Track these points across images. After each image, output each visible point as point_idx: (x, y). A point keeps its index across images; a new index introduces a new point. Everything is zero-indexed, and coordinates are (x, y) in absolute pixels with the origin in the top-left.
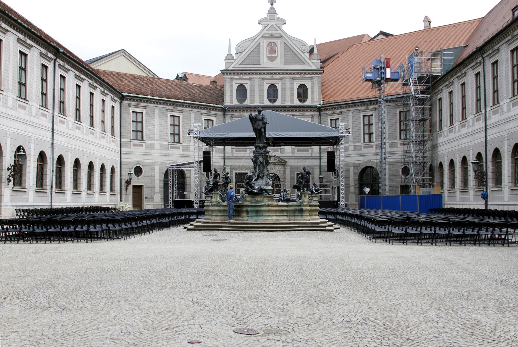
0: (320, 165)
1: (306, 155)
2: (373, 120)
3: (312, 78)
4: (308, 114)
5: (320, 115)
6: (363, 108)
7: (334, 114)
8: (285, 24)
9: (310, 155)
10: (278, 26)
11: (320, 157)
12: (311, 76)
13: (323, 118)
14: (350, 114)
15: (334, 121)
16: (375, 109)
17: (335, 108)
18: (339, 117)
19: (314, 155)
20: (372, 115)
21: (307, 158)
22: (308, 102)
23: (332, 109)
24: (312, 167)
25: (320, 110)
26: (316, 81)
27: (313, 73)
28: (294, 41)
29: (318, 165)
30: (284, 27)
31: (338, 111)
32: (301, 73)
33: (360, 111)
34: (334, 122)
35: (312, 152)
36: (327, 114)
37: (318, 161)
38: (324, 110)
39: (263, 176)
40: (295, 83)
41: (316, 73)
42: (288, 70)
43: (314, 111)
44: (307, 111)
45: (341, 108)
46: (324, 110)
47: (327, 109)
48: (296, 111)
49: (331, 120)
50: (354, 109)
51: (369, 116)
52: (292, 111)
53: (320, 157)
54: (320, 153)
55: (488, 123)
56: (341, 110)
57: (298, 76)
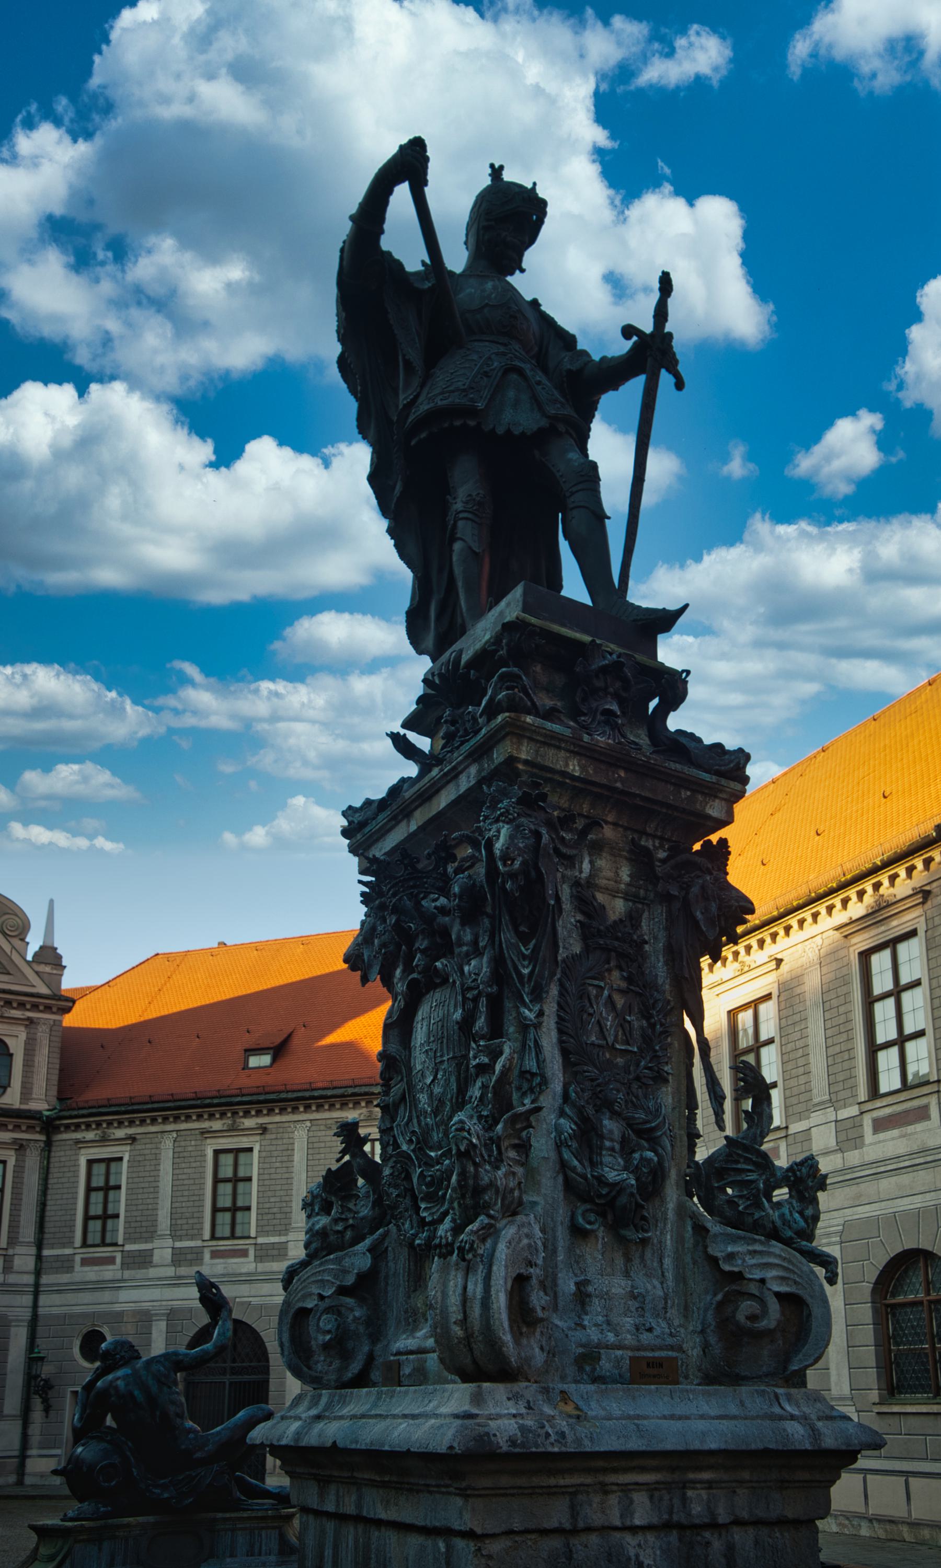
0: (35, 1318)
2: (254, 1166)
6: (217, 1125)
7: (104, 1140)
11: (37, 1285)
14: (167, 1144)
15: (103, 1166)
16: (264, 1130)
17: (110, 1124)
18: (125, 1152)
20: (250, 1150)
23: (99, 1124)
29: (27, 1314)
31: (120, 1133)
33: (205, 1133)
37: (27, 1300)
49: (90, 1162)
50: (184, 1126)
51: (237, 1151)
53: (37, 1285)
54: (38, 1273)
56: (131, 1131)
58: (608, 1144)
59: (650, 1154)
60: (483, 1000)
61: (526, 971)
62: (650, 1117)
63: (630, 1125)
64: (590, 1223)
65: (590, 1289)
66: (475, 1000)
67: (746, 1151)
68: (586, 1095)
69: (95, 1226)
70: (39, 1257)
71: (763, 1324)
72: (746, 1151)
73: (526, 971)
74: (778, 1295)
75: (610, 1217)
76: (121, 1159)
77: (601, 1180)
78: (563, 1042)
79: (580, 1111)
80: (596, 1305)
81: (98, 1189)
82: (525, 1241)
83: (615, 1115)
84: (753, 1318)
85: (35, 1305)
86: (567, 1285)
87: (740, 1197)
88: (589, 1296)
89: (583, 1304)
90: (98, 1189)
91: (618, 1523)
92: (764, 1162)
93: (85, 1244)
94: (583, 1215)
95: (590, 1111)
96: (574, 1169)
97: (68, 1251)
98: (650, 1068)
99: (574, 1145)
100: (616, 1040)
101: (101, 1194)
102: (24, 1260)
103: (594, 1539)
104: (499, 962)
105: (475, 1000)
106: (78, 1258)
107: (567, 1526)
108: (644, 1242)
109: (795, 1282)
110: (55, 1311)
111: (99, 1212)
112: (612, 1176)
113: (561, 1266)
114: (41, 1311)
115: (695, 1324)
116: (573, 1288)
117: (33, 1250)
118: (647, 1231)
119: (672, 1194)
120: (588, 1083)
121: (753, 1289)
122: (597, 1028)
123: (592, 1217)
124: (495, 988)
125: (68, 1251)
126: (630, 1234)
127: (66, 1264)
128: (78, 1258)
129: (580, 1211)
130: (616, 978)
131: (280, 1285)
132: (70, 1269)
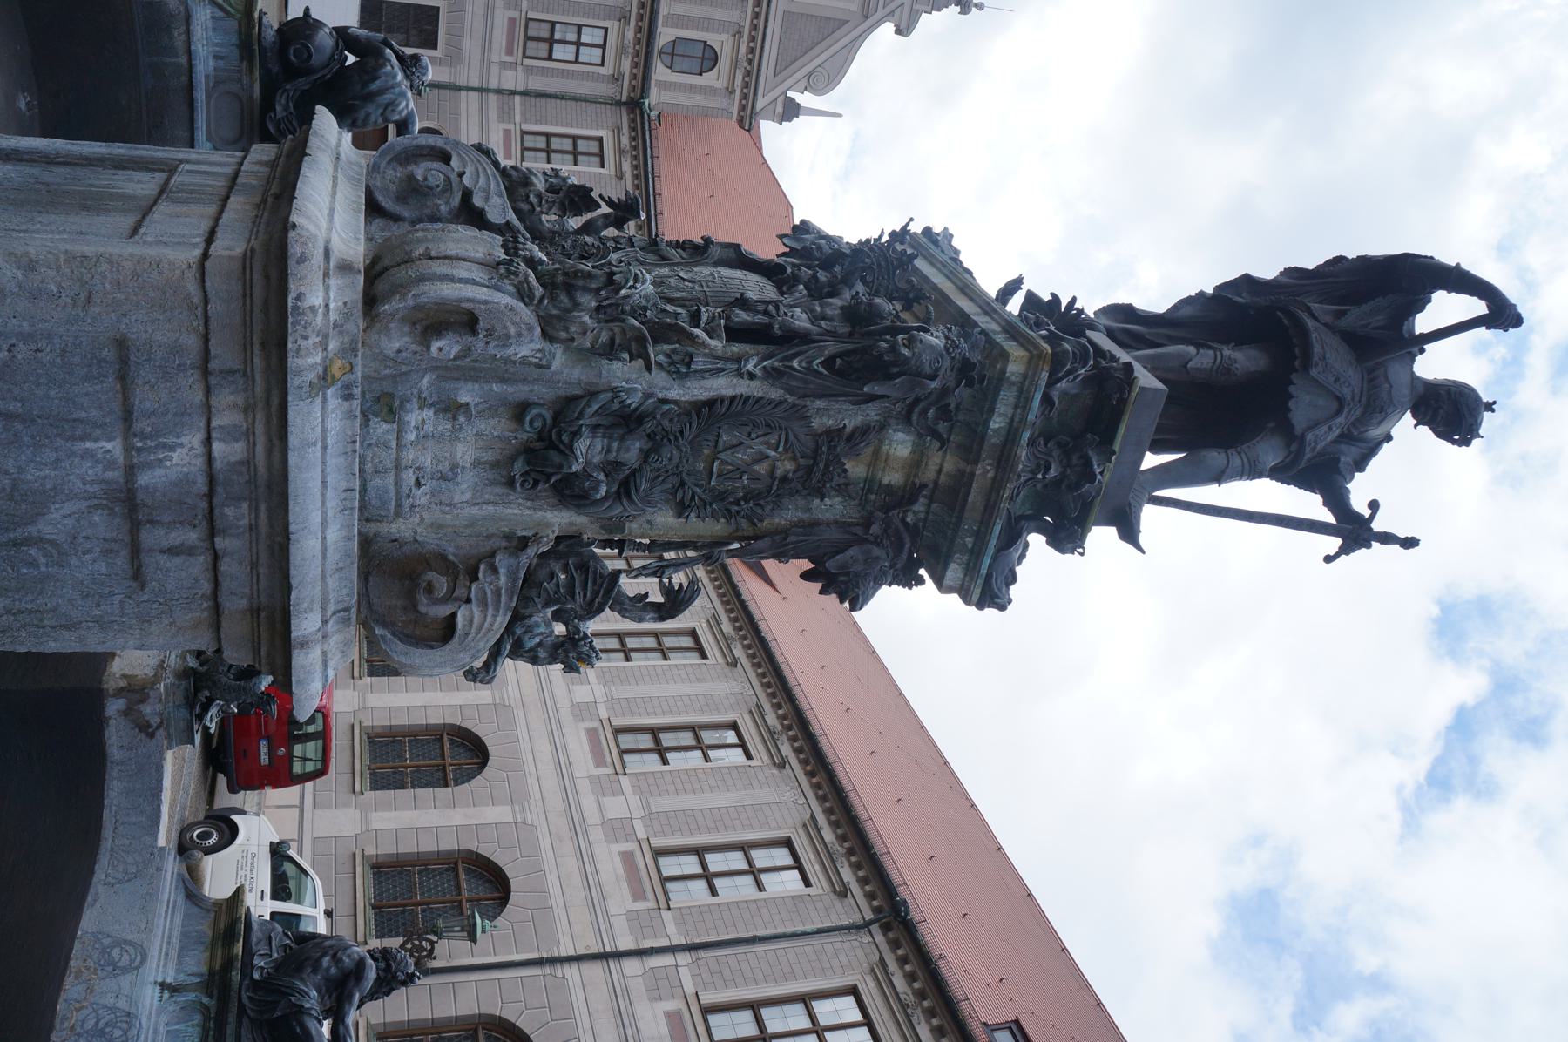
0: (459, 88)
1: (495, 46)
3: (733, 92)
4: (626, 66)
5: (619, 104)
7: (620, 152)
8: (899, 31)
9: (495, 58)
10: (897, 12)
11: (487, 90)
12: (738, 91)
13: (609, 111)
17: (636, 158)
19: (495, 69)
21: (486, 47)
22: (660, 72)
23: (635, 148)
24: (454, 58)
25: (635, 105)
26: (721, 102)
27: (745, 96)
28: (845, 51)
29: (461, 82)
30: (888, 28)
32: (750, 62)
34: (593, 147)
35: (503, 65)
36: (619, 129)
37: (475, 83)
38: (634, 120)
39: (571, 492)
40: (724, 37)
41: (743, 108)
42: (767, 20)
43: (633, 88)
44: (635, 65)
45: (636, 177)
46: (634, 120)
47: (634, 129)
48: (639, 30)
49: (600, 140)
52: (641, 18)
53: (487, 90)
54: (499, 92)
55: (632, 966)
57: (743, 49)
58: (615, 445)
59: (603, 490)
60: (766, 320)
61: (795, 364)
62: (642, 494)
63: (633, 473)
64: (531, 422)
65: (462, 419)
66: (766, 313)
67: (605, 592)
68: (666, 423)
69: (540, 142)
70: (513, 93)
71: (422, 598)
72: (605, 592)
73: (795, 364)
74: (453, 616)
75: (538, 445)
76: (602, 166)
77: (576, 434)
78: (722, 401)
79: (652, 415)
80: (445, 426)
81: (575, 145)
82: (513, 331)
83: (645, 456)
84: (430, 589)
85: (469, 89)
86: (467, 394)
87: (558, 585)
88: (455, 418)
89: (446, 410)
90: (575, 145)
91: (214, 423)
92: (592, 611)
93: (524, 133)
94: (540, 415)
95: (649, 426)
96: (588, 405)
97: (518, 118)
98: (693, 498)
99: (616, 406)
100: (724, 463)
101: (570, 148)
102: (512, 80)
103: (199, 397)
104: (803, 338)
105: (766, 313)
106: (511, 126)
107: (213, 365)
108: (510, 483)
109: (467, 634)
110: (463, 106)
111: (553, 146)
112: (581, 446)
113: (487, 387)
114: (463, 94)
115: (424, 535)
116: (463, 399)
117: (520, 88)
118: (522, 486)
119: (559, 520)
120: (677, 428)
121: (460, 592)
122: (735, 442)
123: (538, 424)
124: (779, 333)
125: (518, 118)
126: (519, 467)
127: (505, 115)
128: (511, 126)
129: (544, 412)
130: (785, 466)
131: (475, 141)
132: (501, 119)
